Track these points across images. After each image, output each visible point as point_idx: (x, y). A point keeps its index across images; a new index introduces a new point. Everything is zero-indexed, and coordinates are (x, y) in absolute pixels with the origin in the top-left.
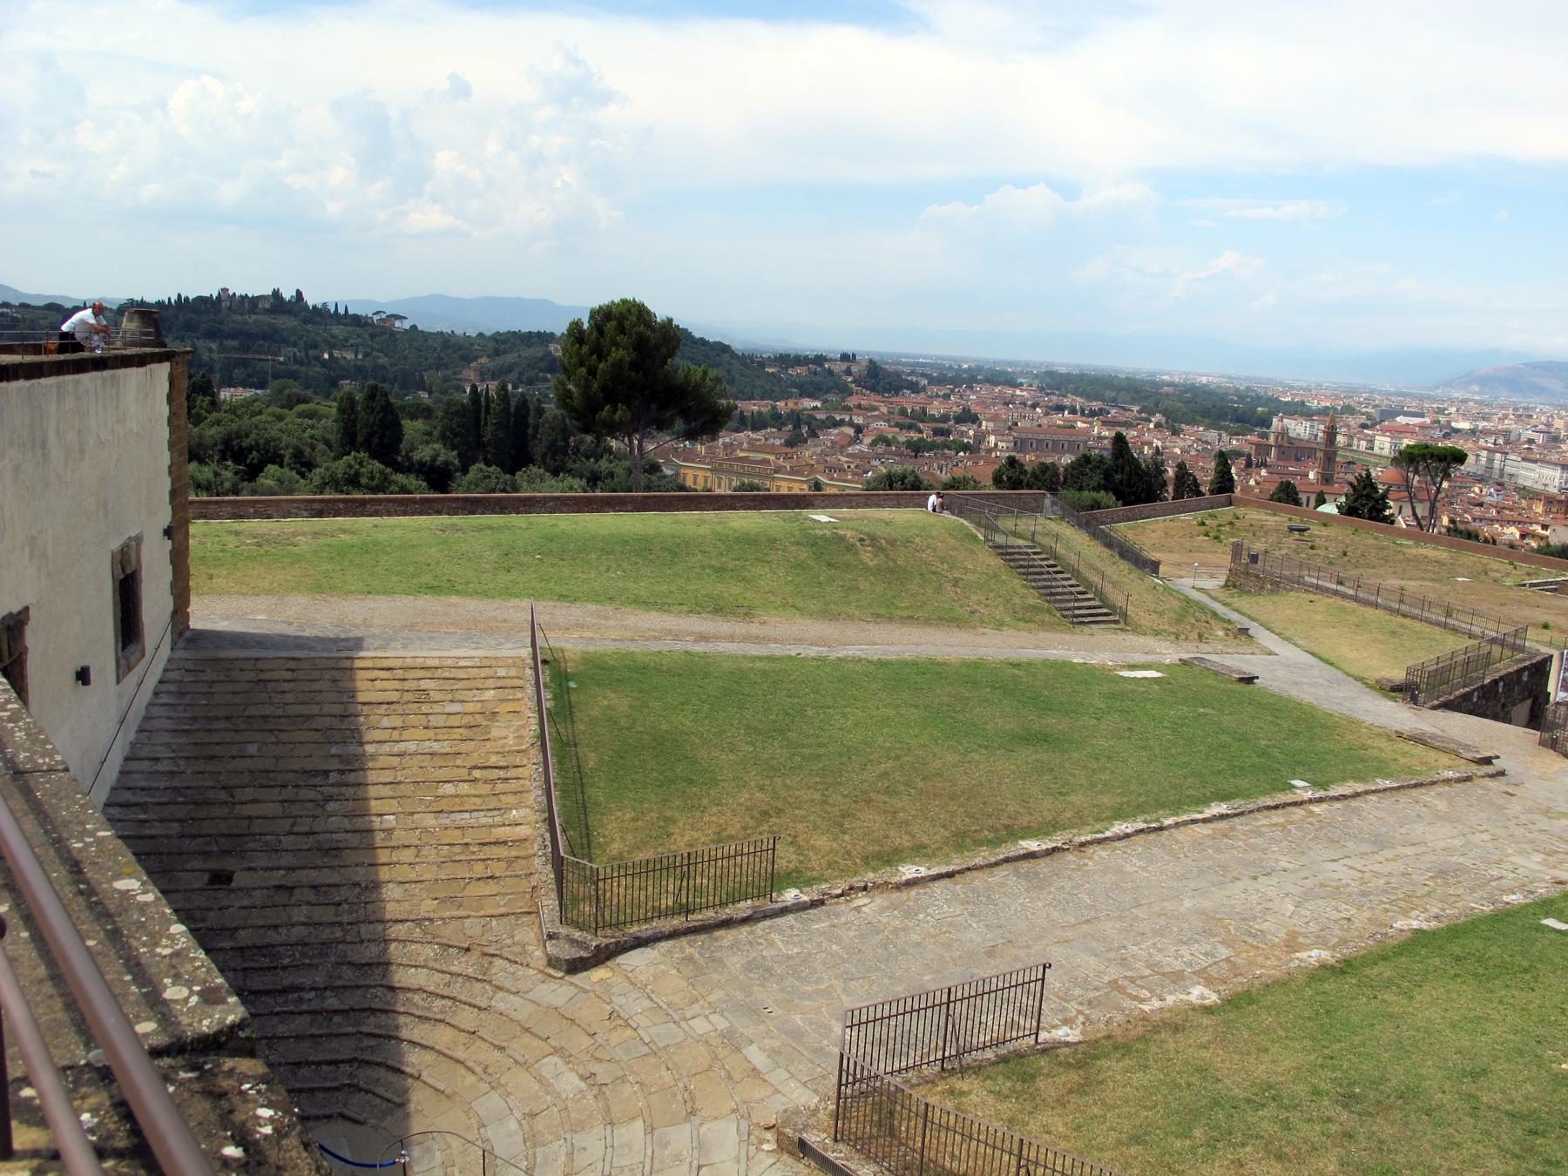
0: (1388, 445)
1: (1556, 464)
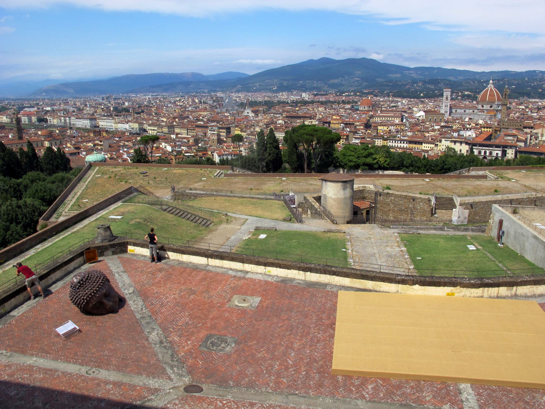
0: (27, 120)
1: (87, 119)
